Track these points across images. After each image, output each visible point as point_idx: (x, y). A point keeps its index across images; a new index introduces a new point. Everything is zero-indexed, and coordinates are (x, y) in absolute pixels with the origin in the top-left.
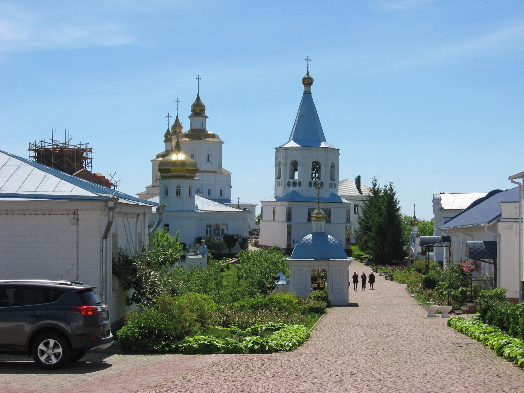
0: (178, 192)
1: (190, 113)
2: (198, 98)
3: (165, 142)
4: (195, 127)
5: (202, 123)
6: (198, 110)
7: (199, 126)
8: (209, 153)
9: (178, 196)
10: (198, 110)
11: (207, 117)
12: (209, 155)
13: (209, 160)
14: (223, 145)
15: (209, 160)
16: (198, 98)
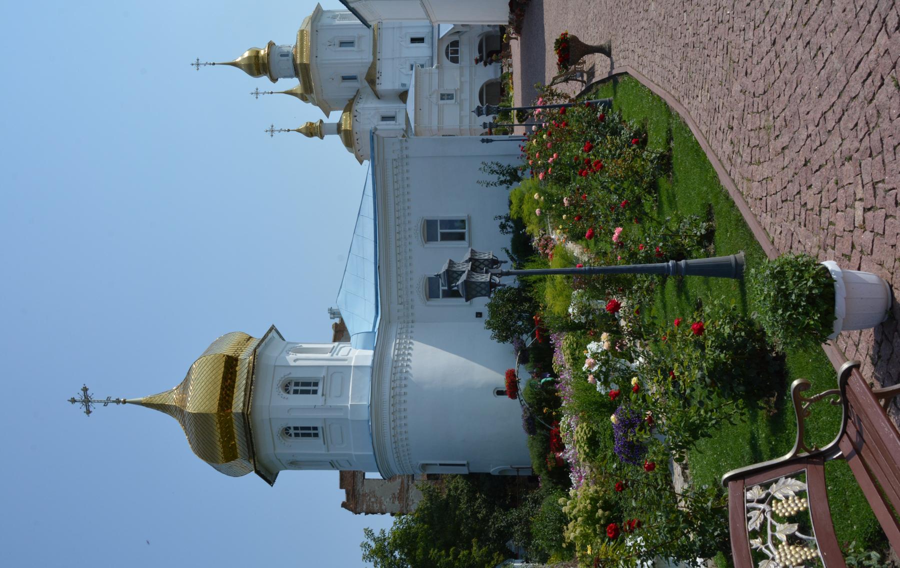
0: (308, 432)
1: (265, 79)
2: (234, 64)
3: (322, 137)
4: (292, 71)
5: (282, 56)
6: (258, 66)
7: (288, 64)
8: (337, 43)
9: (320, 432)
10: (258, 66)
11: (271, 45)
12: (342, 44)
13: (351, 43)
14: (324, 8)
15: (351, 43)
16: (234, 64)
